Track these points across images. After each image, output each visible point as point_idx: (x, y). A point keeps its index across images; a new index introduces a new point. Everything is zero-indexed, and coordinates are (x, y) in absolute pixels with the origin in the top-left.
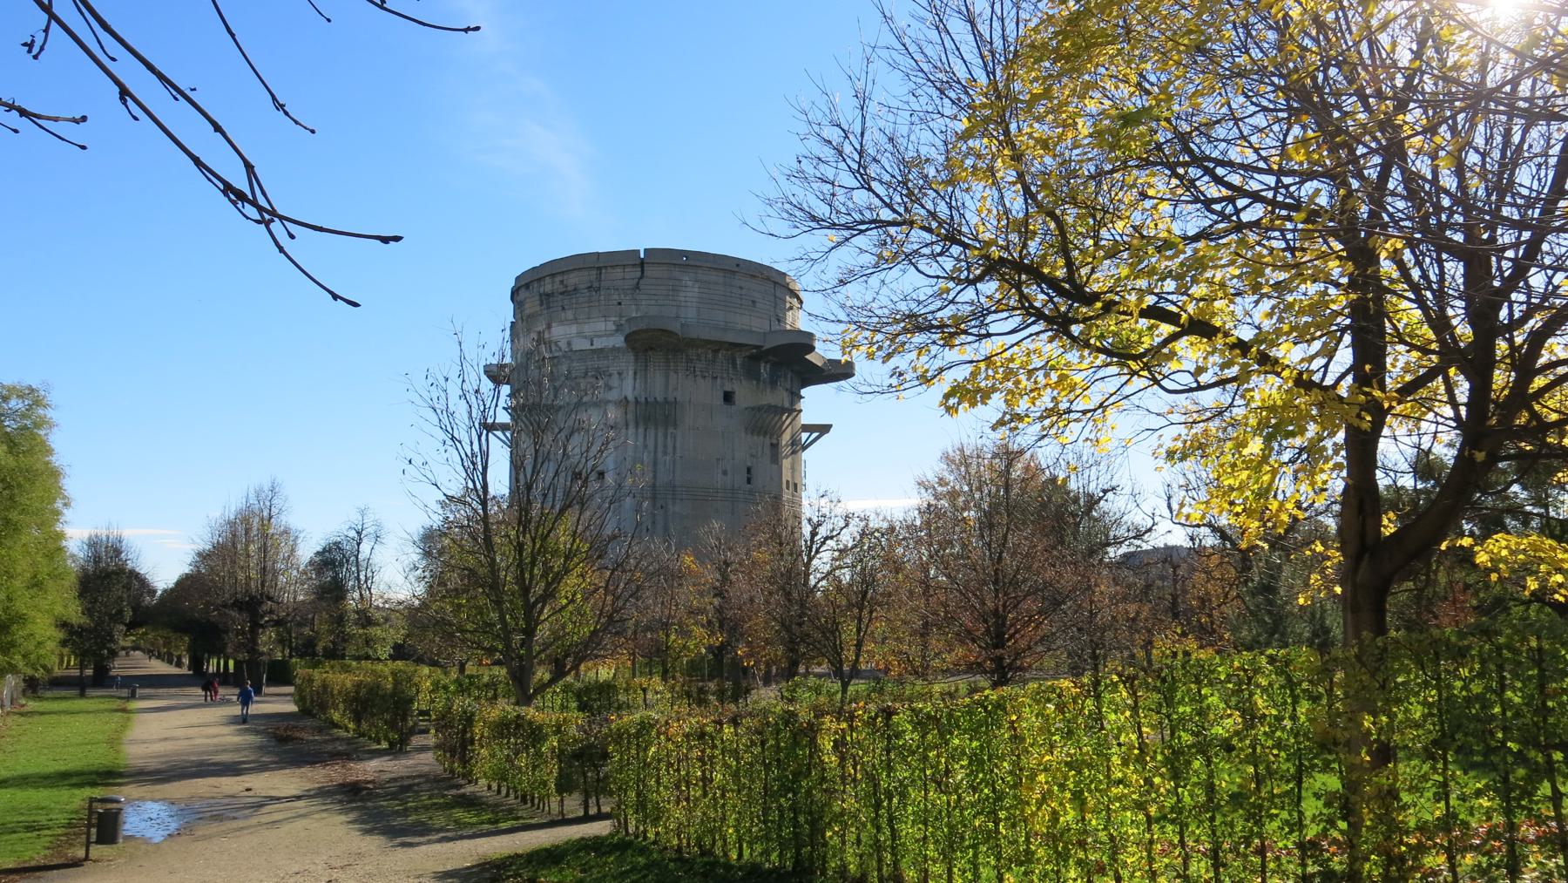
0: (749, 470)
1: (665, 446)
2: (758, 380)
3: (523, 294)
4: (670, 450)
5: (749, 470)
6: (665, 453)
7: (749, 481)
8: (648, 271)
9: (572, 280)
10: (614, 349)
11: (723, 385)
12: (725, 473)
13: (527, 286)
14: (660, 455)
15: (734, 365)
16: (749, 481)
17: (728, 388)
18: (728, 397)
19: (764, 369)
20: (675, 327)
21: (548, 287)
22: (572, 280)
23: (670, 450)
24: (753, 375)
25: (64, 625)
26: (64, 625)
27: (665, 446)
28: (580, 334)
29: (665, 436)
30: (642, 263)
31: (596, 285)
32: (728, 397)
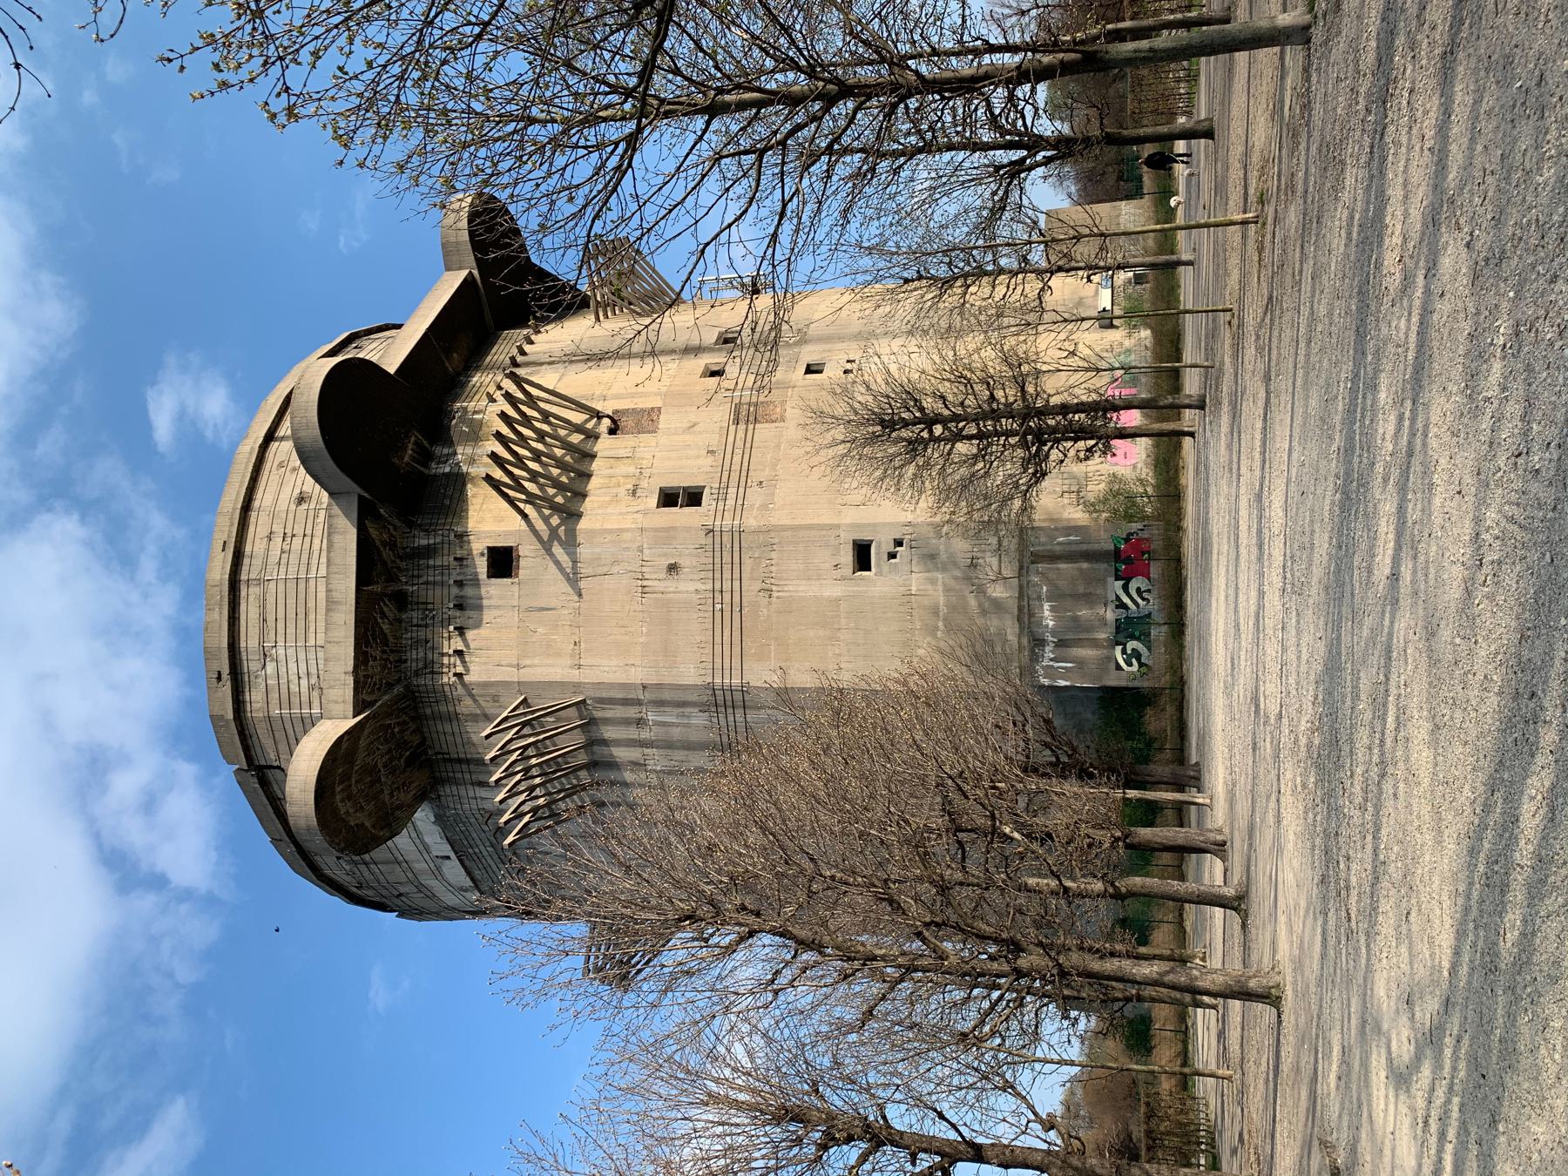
0: (669, 498)
1: (626, 722)
4: (632, 712)
5: (669, 498)
6: (640, 722)
7: (694, 498)
10: (440, 820)
14: (645, 735)
15: (430, 552)
16: (694, 498)
17: (482, 566)
18: (502, 562)
23: (632, 712)
27: (626, 722)
28: (438, 873)
29: (606, 721)
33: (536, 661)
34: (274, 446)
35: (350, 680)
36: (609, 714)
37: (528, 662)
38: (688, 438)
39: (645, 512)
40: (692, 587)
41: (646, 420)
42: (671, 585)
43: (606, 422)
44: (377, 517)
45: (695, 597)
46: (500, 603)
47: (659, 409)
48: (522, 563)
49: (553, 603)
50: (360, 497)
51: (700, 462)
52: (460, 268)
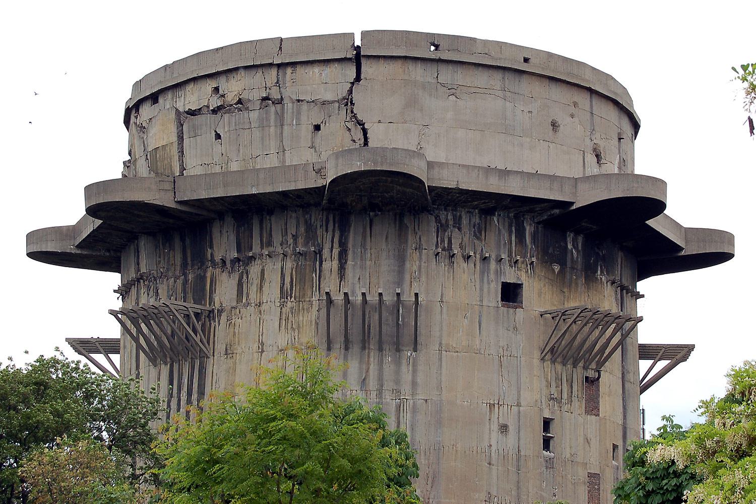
0: (547, 424)
2: (563, 264)
3: (146, 111)
5: (547, 424)
8: (367, 68)
9: (233, 88)
11: (499, 273)
12: (504, 428)
13: (154, 98)
18: (511, 294)
19: (573, 246)
20: (416, 169)
21: (191, 98)
22: (233, 88)
24: (551, 255)
25: (113, 313)
26: (113, 313)
30: (358, 58)
31: (275, 95)
32: (511, 294)
33: (444, 316)
34: (587, 95)
35: (452, 185)
36: (404, 368)
37: (445, 311)
38: (581, 440)
39: (541, 410)
40: (494, 443)
41: (592, 407)
42: (495, 427)
43: (591, 374)
44: (553, 208)
45: (487, 444)
46: (485, 290)
47: (598, 415)
48: (511, 310)
49: (484, 333)
50: (572, 203)
51: (568, 450)
52: (687, 242)
